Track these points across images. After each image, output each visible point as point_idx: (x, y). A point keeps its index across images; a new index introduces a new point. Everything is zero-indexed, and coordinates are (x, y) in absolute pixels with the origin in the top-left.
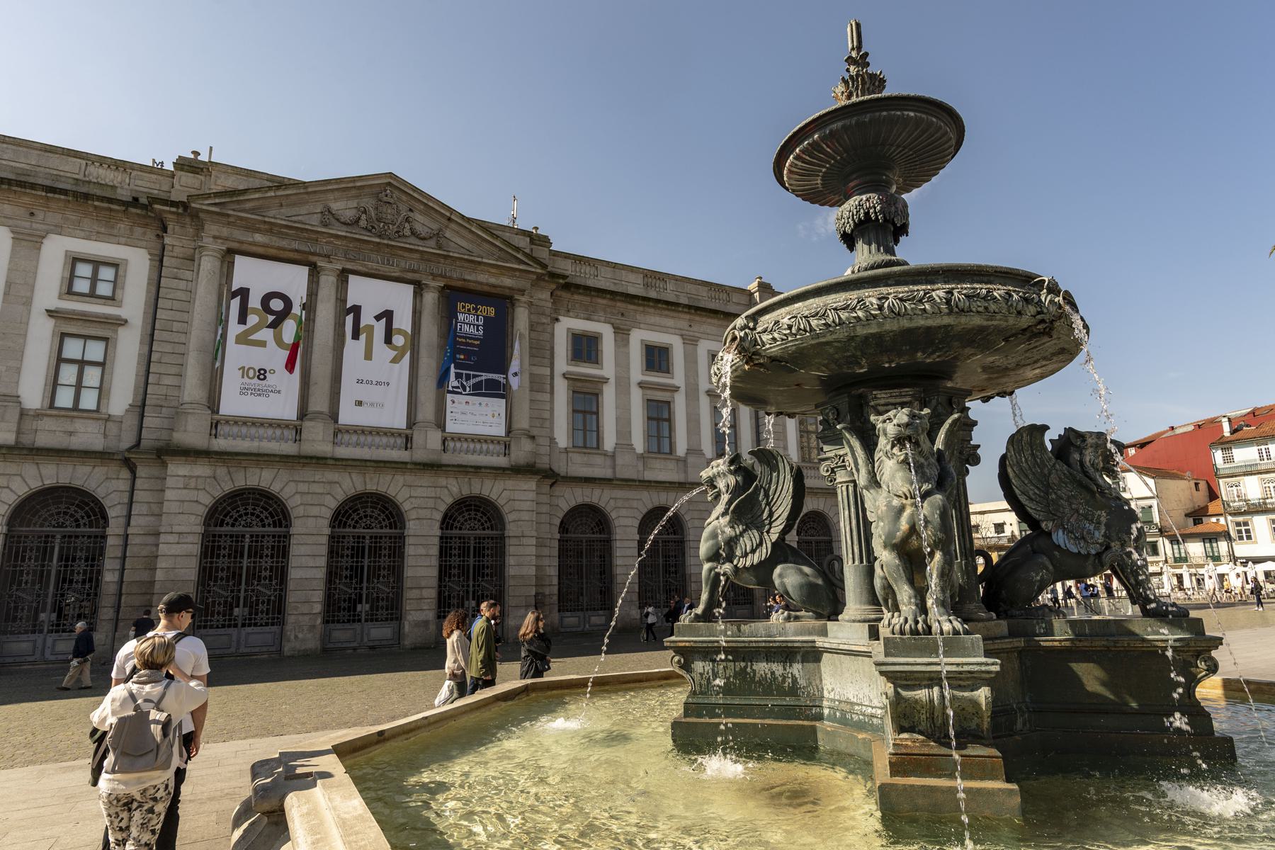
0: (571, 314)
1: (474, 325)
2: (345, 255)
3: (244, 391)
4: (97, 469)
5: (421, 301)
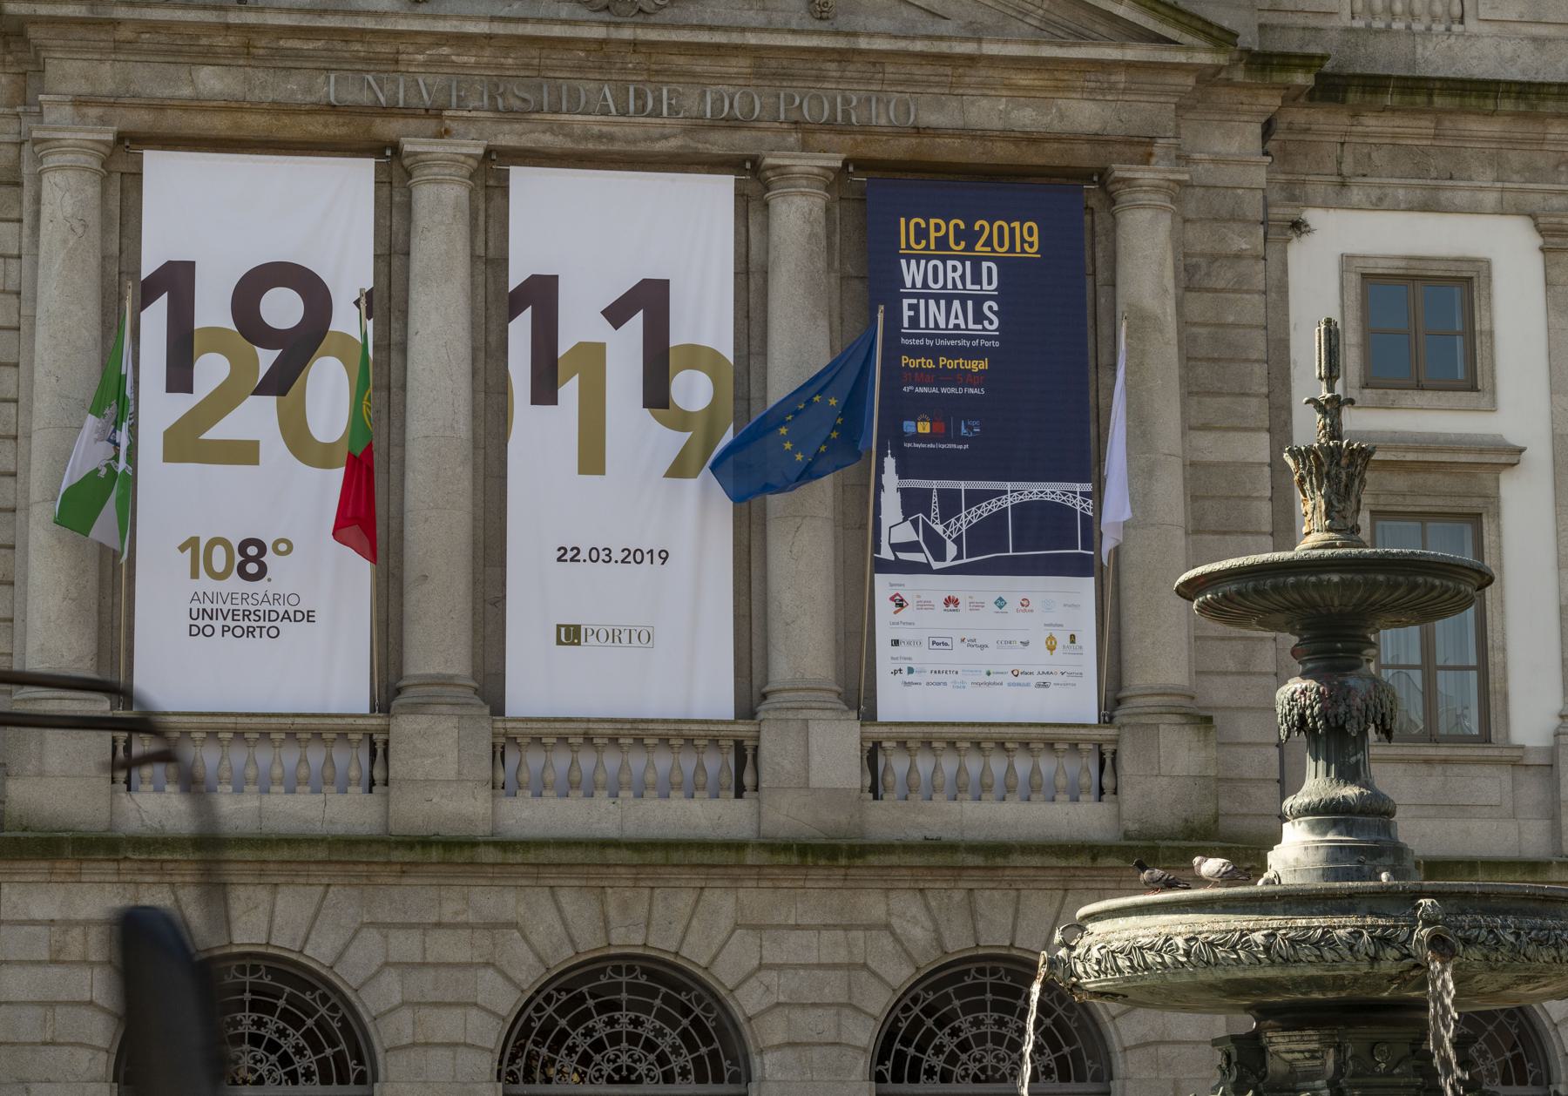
0: (1356, 195)
1: (963, 299)
2: (492, 98)
3: (202, 621)
5: (766, 228)
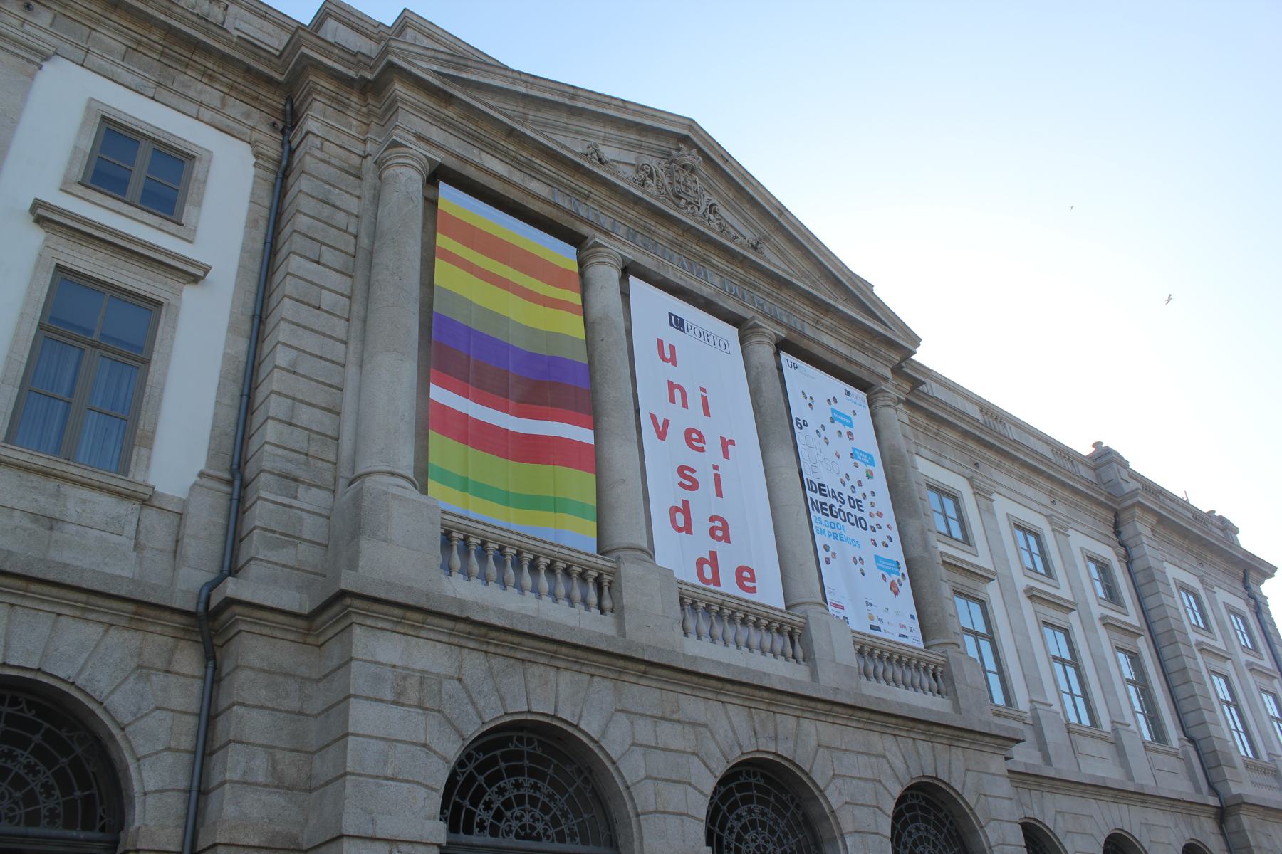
4: (113, 632)
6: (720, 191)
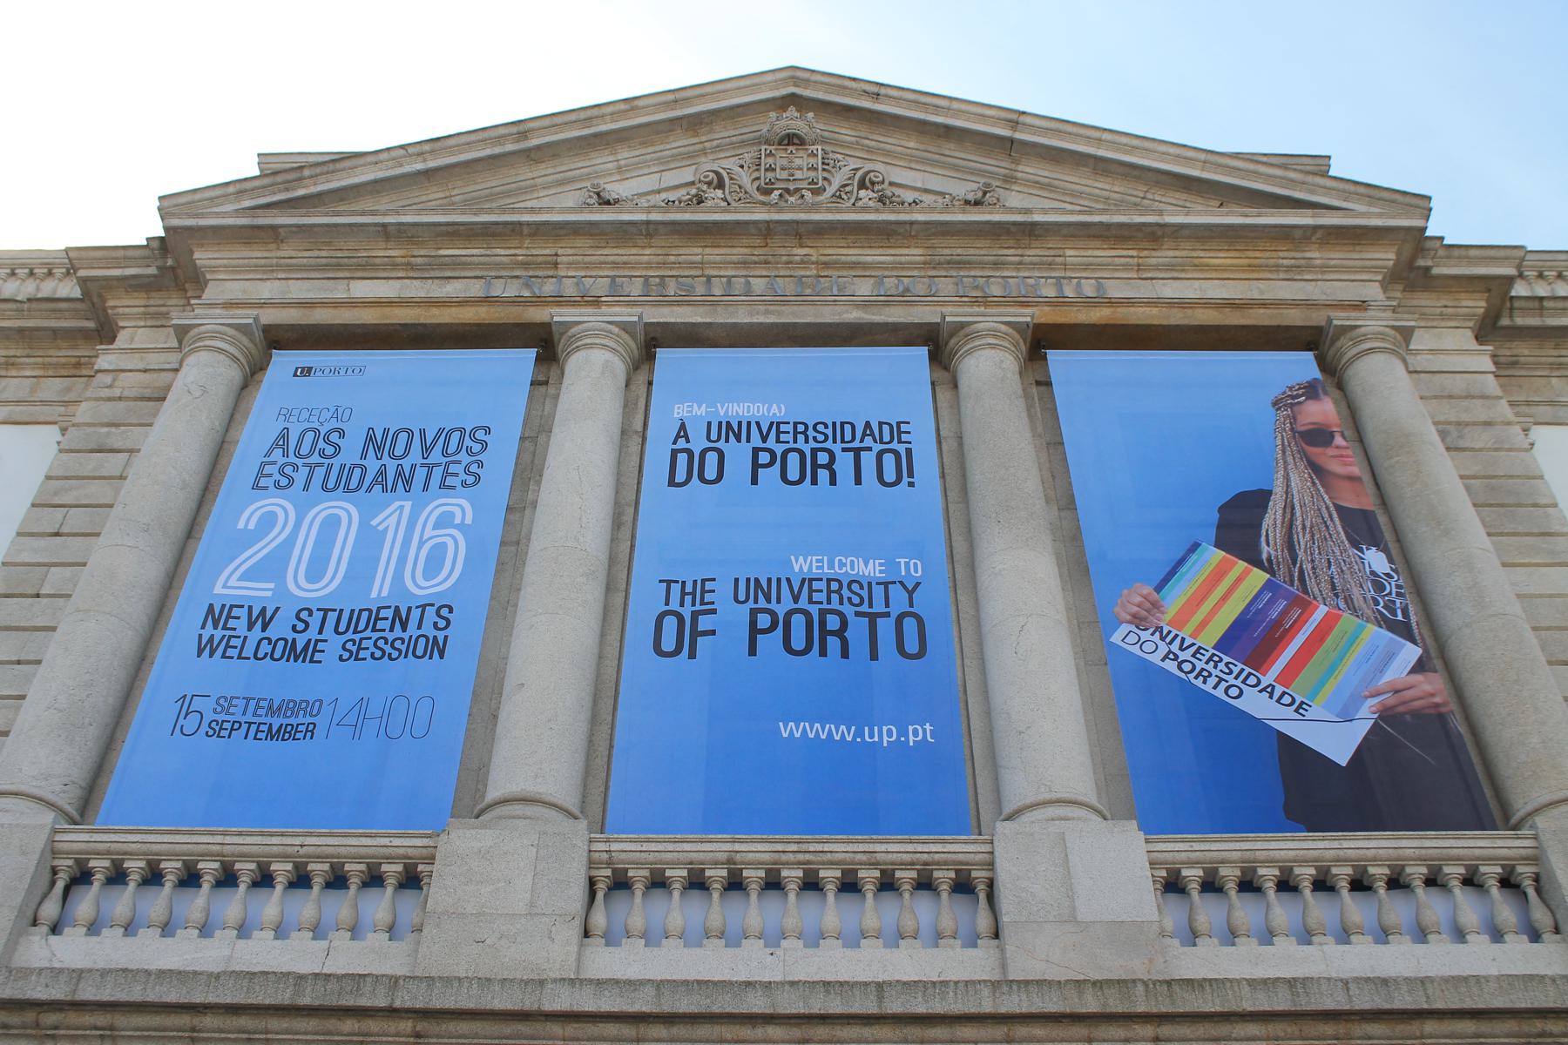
6: (888, 147)
